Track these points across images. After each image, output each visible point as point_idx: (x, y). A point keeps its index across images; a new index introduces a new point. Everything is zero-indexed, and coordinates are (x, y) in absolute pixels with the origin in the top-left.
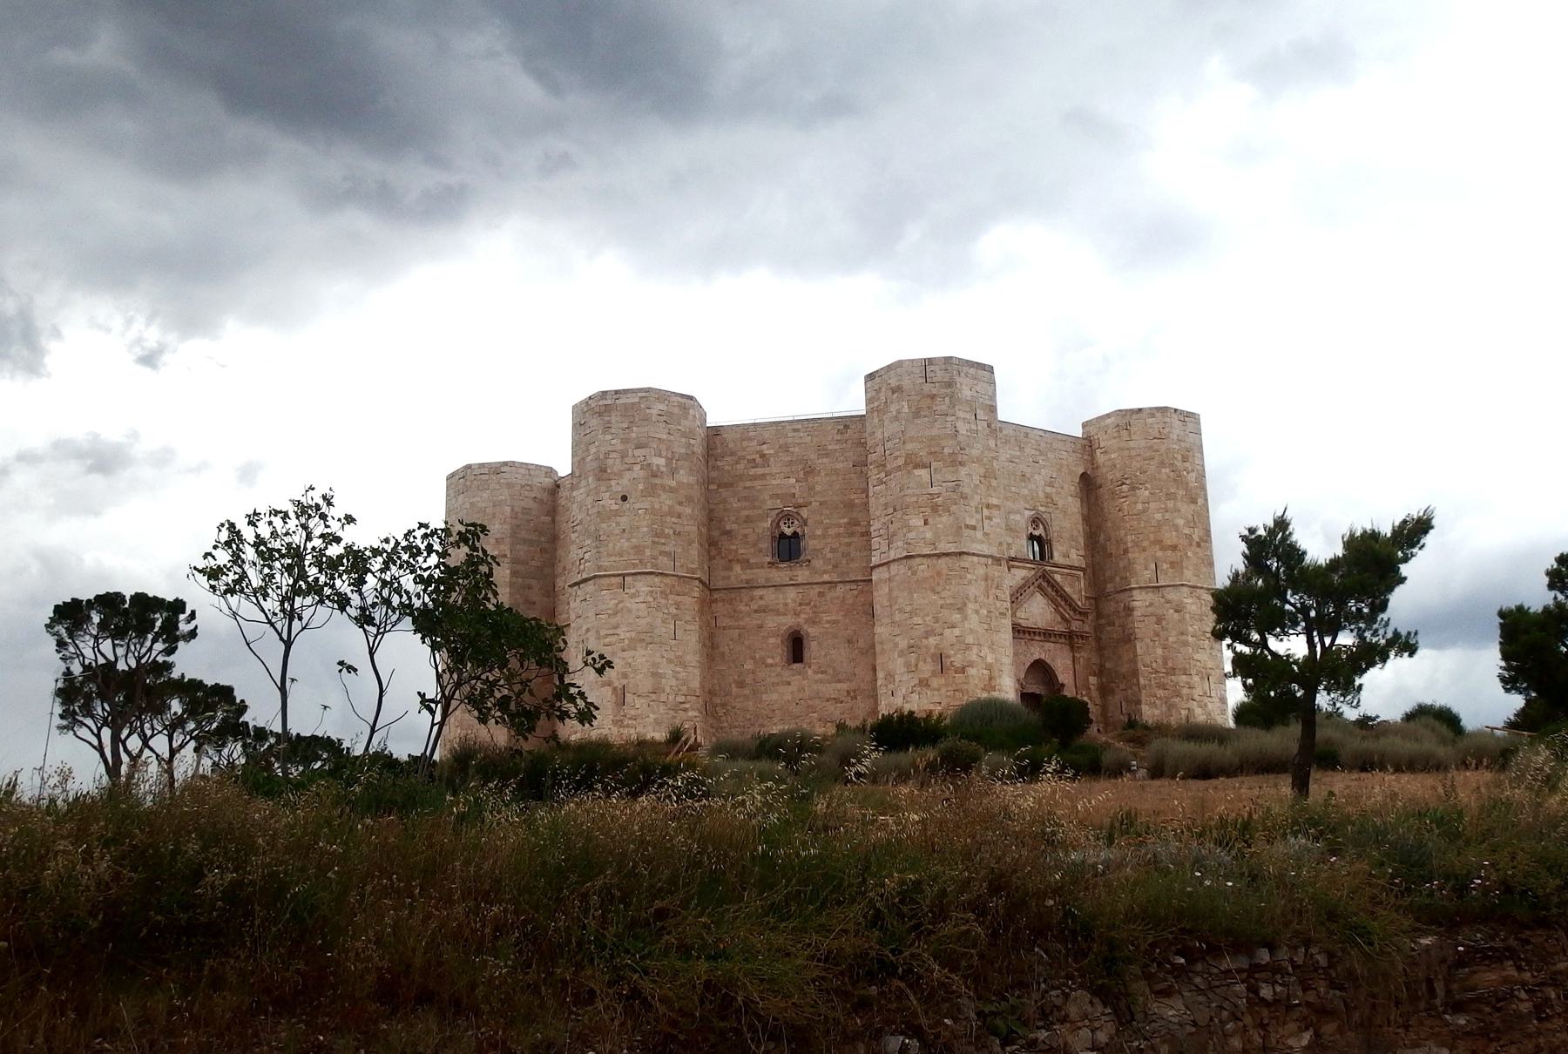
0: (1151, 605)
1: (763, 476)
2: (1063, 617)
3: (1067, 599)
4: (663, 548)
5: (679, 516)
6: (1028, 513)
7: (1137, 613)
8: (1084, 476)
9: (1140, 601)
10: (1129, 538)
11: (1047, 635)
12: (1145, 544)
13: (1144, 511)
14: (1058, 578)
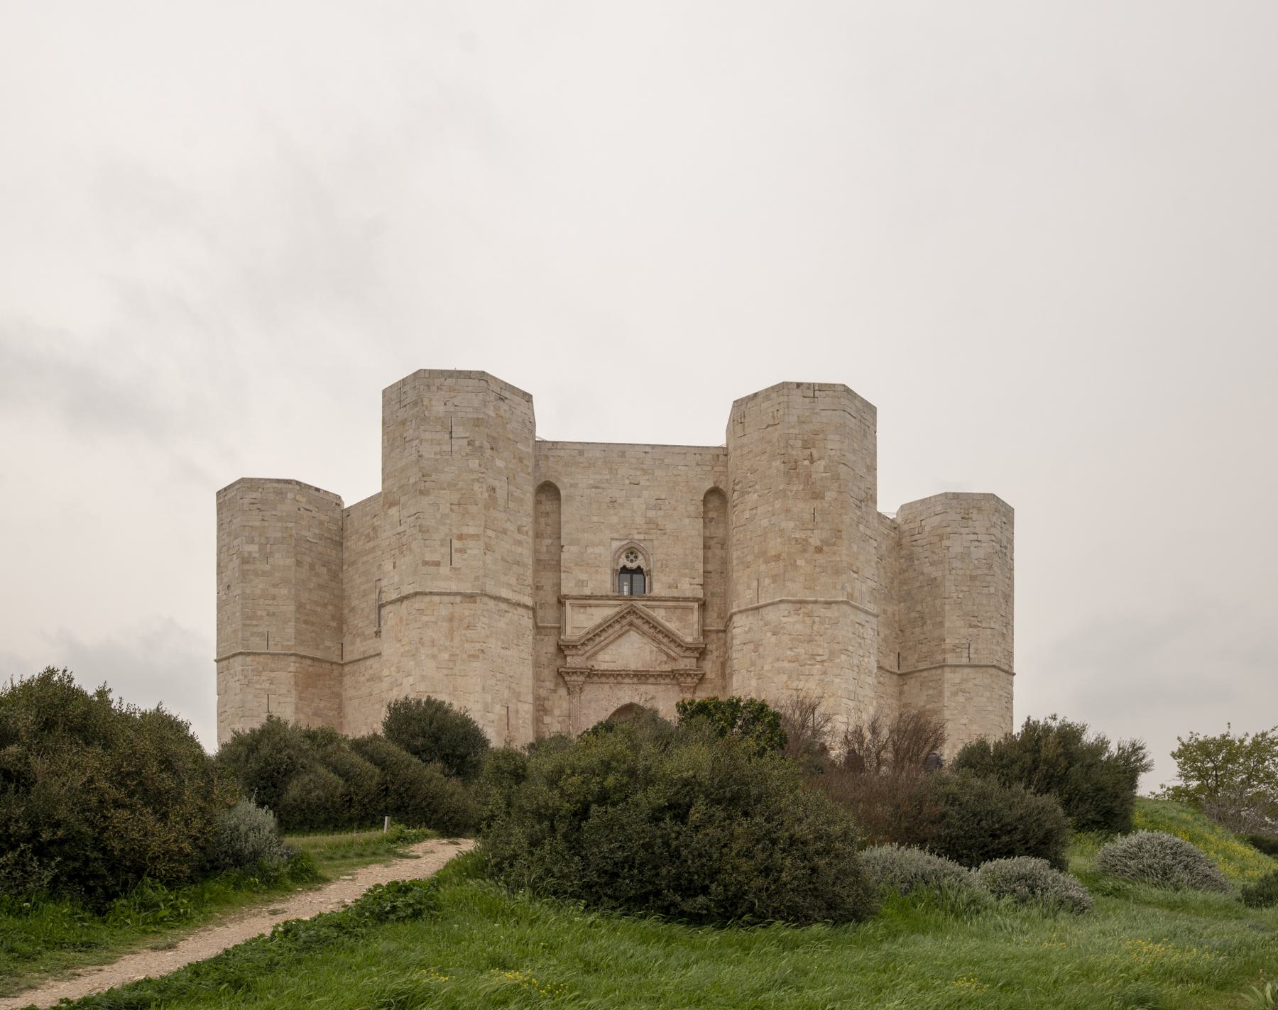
0: (750, 629)
1: (373, 549)
2: (667, 654)
3: (668, 635)
4: (255, 629)
5: (274, 598)
6: (616, 544)
7: (736, 642)
8: (715, 492)
9: (742, 627)
10: (735, 555)
11: (641, 676)
12: (750, 558)
13: (751, 519)
14: (659, 615)
